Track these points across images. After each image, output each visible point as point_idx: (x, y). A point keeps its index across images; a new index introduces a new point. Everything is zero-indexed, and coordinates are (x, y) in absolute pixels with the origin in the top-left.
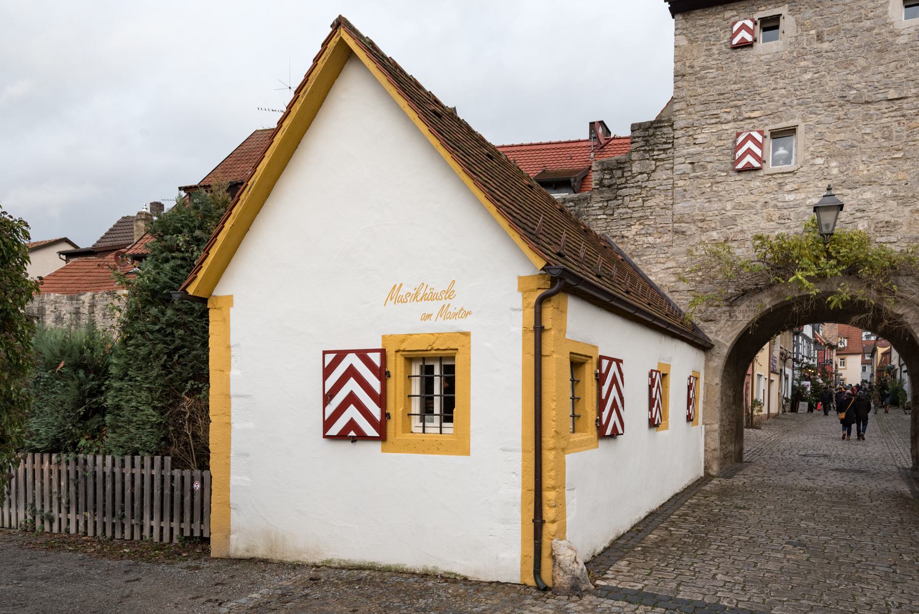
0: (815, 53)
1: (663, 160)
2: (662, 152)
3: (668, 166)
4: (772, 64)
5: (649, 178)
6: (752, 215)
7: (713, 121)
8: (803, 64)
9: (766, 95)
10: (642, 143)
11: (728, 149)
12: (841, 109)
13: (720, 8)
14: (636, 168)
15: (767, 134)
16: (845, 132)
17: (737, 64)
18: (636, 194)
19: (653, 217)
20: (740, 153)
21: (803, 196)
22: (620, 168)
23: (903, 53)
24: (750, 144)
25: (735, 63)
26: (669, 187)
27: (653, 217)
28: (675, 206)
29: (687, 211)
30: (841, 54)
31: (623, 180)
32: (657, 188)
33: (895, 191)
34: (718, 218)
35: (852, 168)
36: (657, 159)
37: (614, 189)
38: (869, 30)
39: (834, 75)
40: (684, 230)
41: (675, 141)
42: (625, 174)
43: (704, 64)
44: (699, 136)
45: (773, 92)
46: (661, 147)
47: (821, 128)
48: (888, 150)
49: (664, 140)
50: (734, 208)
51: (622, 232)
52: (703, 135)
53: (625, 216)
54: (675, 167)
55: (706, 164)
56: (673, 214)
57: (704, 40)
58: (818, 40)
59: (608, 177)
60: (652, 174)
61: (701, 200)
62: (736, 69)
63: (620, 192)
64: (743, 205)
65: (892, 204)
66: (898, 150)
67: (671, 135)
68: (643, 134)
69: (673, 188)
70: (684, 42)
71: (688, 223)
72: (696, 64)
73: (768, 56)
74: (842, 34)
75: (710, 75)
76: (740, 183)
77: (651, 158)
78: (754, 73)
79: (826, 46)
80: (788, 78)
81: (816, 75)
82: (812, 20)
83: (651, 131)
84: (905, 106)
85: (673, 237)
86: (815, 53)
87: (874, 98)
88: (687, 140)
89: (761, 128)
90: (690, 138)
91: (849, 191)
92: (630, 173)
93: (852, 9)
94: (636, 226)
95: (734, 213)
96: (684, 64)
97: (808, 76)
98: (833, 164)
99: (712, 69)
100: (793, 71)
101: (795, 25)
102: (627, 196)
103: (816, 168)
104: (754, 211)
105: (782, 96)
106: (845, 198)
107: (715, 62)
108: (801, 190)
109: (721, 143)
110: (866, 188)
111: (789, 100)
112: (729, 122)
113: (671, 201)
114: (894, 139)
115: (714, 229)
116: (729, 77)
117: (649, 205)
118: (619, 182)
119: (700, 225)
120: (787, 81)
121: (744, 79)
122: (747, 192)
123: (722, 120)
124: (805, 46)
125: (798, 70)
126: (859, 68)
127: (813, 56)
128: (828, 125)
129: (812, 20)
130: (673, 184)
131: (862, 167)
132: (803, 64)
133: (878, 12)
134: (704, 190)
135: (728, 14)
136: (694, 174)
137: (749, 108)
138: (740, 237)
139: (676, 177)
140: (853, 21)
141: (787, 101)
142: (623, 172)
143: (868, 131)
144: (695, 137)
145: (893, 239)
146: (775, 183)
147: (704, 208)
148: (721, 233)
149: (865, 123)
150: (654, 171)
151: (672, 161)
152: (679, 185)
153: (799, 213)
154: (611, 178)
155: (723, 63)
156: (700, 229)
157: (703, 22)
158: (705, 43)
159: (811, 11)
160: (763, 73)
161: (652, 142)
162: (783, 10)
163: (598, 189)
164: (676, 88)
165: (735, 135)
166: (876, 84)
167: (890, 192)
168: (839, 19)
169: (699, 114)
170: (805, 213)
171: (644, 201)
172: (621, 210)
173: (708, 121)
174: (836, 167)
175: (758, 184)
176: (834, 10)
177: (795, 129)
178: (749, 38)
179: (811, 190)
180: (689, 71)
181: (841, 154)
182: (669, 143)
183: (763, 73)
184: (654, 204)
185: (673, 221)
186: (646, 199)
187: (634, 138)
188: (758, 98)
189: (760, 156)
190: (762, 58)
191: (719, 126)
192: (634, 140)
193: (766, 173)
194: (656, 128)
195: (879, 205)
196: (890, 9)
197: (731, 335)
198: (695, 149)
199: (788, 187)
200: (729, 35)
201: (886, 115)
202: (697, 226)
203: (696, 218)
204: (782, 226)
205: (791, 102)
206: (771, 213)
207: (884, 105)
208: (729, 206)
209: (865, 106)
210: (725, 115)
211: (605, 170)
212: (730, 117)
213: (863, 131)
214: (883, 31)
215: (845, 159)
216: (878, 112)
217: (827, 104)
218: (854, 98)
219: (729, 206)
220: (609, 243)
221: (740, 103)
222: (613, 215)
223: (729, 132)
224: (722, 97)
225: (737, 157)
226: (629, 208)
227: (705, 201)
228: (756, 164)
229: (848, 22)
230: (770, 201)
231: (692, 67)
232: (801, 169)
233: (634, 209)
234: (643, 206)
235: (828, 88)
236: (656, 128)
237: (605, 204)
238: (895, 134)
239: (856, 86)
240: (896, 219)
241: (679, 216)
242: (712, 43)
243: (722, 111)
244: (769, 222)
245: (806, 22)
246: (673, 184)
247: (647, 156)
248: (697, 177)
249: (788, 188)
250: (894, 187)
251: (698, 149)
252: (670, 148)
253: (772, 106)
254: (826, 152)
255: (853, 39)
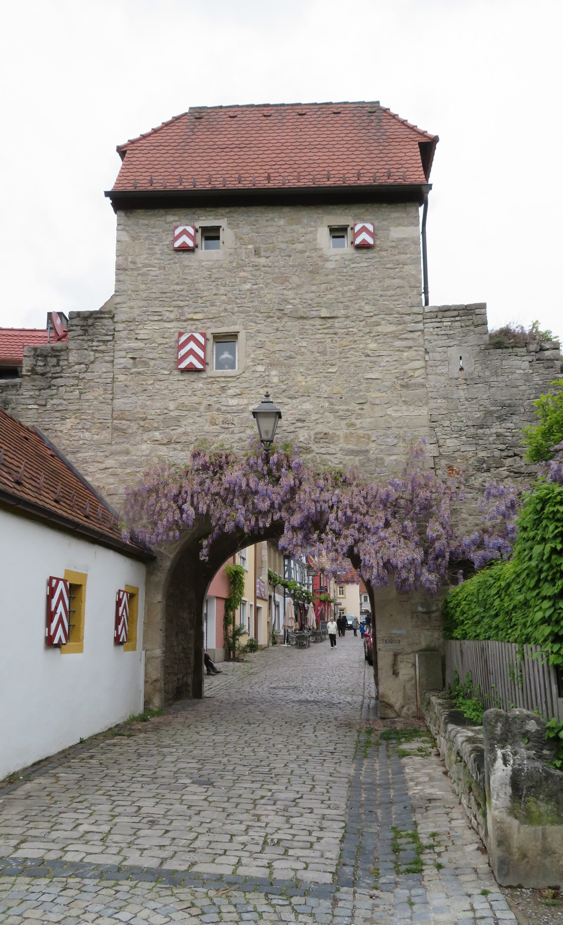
0: (253, 266)
1: (103, 352)
2: (102, 344)
3: (107, 358)
4: (213, 270)
5: (87, 369)
6: (195, 417)
7: (156, 318)
8: (242, 274)
9: (208, 298)
10: (80, 332)
11: (171, 347)
12: (279, 321)
13: (162, 211)
14: (73, 357)
15: (210, 336)
16: (283, 343)
17: (180, 266)
18: (73, 386)
19: (91, 412)
20: (183, 352)
21: (246, 401)
22: (56, 356)
23: (331, 277)
24: (192, 345)
25: (177, 265)
26: (109, 381)
27: (91, 412)
28: (115, 401)
29: (127, 408)
30: (277, 270)
31: (58, 369)
32: (95, 380)
33: (331, 404)
34: (161, 417)
35: (291, 378)
36: (96, 350)
37: (47, 378)
38: (302, 252)
39: (271, 289)
40: (124, 427)
41: (116, 333)
42: (61, 363)
43: (147, 261)
44: (141, 332)
45: (215, 297)
46: (101, 338)
47: (261, 337)
48: (324, 364)
49: (104, 331)
50: (177, 409)
51: (56, 426)
52: (145, 331)
53: (60, 408)
54: (116, 361)
55: (148, 360)
56: (113, 410)
57: (146, 239)
58: (255, 254)
59: (41, 364)
60: (91, 366)
61: (143, 397)
62: (178, 270)
63: (54, 382)
64: (186, 406)
65: (330, 417)
66: (332, 365)
67: (112, 328)
68: (81, 323)
69: (113, 382)
70: (126, 238)
71: (128, 420)
72: (138, 260)
73: (209, 263)
74: (277, 252)
75: (152, 273)
76: (183, 383)
77: (90, 348)
78: (196, 277)
79: (262, 261)
80: (229, 286)
81: (255, 287)
82: (250, 235)
83: (90, 321)
84: (337, 325)
85: (112, 435)
86: (253, 266)
87: (308, 314)
88: (128, 334)
89: (203, 331)
90: (132, 332)
91: (289, 400)
92: (66, 363)
93: (285, 231)
94: (72, 420)
95: (176, 413)
96: (126, 259)
97: (248, 286)
98: (274, 373)
99: (154, 267)
100: (233, 280)
101: (234, 238)
102: (62, 386)
103: (257, 375)
104: (197, 413)
105: (224, 302)
106: (286, 407)
107: (157, 261)
108: (243, 396)
109: (164, 341)
110: (305, 399)
111: (231, 306)
112: (172, 321)
113: (111, 396)
114: (328, 354)
115: (157, 429)
116: (171, 277)
117: (87, 397)
118: (54, 370)
119: (142, 423)
120: (228, 288)
121: (187, 281)
122: (190, 393)
123: (165, 318)
124: (243, 258)
125: (238, 280)
126: (294, 285)
127: (251, 269)
128: (267, 335)
129: (250, 235)
130: (113, 378)
131: (300, 378)
132: (242, 274)
133: (309, 237)
134: (145, 387)
135: (170, 218)
136: (136, 370)
137: (191, 310)
138: (183, 439)
139: (116, 371)
140: (286, 242)
141: (228, 307)
142: (59, 361)
143: (304, 344)
144: (137, 332)
145: (331, 451)
146: (218, 386)
147: (146, 406)
148: (164, 433)
149: (301, 337)
150: (92, 362)
151: (112, 354)
152: (119, 380)
153: (242, 418)
154: (45, 365)
155: (166, 263)
156: (142, 428)
157: (146, 222)
158: (147, 242)
159: (248, 228)
160: (204, 278)
161: (90, 332)
162: (222, 222)
163: (29, 376)
164: (118, 281)
165: (177, 334)
166: (310, 302)
167: (327, 404)
168: (274, 239)
169: (141, 309)
170: (248, 419)
171: (81, 393)
172: (55, 401)
173: (150, 318)
174: (276, 375)
175: (201, 385)
176: (269, 229)
177: (237, 335)
178: (191, 244)
179: (253, 396)
180: (131, 266)
181: (280, 364)
182: (109, 335)
183: (204, 278)
184: (92, 397)
185: (112, 417)
186: (83, 391)
187: (72, 326)
188: (200, 301)
189: (203, 357)
190: (204, 263)
191: (161, 323)
192: (72, 328)
193: (209, 375)
194: (96, 318)
195: (318, 416)
196: (319, 236)
197: (174, 546)
198: (136, 344)
199: (231, 392)
200: (171, 238)
201: (320, 332)
202: (139, 424)
203: (137, 416)
204: (226, 431)
205: (232, 308)
206: (216, 416)
207: (318, 322)
208: (172, 406)
209: (301, 321)
210: (167, 313)
211: (38, 356)
212: (172, 316)
213: (300, 344)
214: (314, 255)
215: (284, 370)
216: (313, 328)
217: (266, 314)
218: (291, 312)
219: (172, 406)
220: (39, 437)
221: (182, 304)
222: (45, 405)
223: (172, 331)
224: (164, 296)
225: (179, 357)
226: (64, 400)
227: (147, 398)
228: (199, 366)
229: (282, 242)
230: (213, 404)
231: (134, 263)
232: (243, 375)
233: (70, 401)
234: (80, 399)
235: (266, 300)
236: (96, 318)
237: (37, 393)
238: (329, 350)
239: (292, 301)
240: (334, 431)
241: (119, 413)
242: (154, 243)
243: (165, 309)
244: (213, 425)
245: (244, 237)
246: (113, 378)
247: (85, 345)
248: (139, 373)
249: (231, 392)
250: (331, 400)
251: (140, 344)
252: (110, 341)
253: (214, 310)
254: (267, 361)
255: (287, 258)
